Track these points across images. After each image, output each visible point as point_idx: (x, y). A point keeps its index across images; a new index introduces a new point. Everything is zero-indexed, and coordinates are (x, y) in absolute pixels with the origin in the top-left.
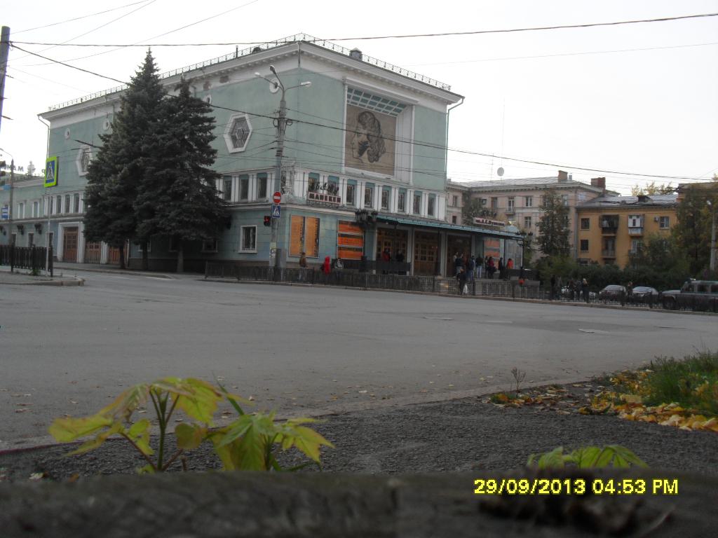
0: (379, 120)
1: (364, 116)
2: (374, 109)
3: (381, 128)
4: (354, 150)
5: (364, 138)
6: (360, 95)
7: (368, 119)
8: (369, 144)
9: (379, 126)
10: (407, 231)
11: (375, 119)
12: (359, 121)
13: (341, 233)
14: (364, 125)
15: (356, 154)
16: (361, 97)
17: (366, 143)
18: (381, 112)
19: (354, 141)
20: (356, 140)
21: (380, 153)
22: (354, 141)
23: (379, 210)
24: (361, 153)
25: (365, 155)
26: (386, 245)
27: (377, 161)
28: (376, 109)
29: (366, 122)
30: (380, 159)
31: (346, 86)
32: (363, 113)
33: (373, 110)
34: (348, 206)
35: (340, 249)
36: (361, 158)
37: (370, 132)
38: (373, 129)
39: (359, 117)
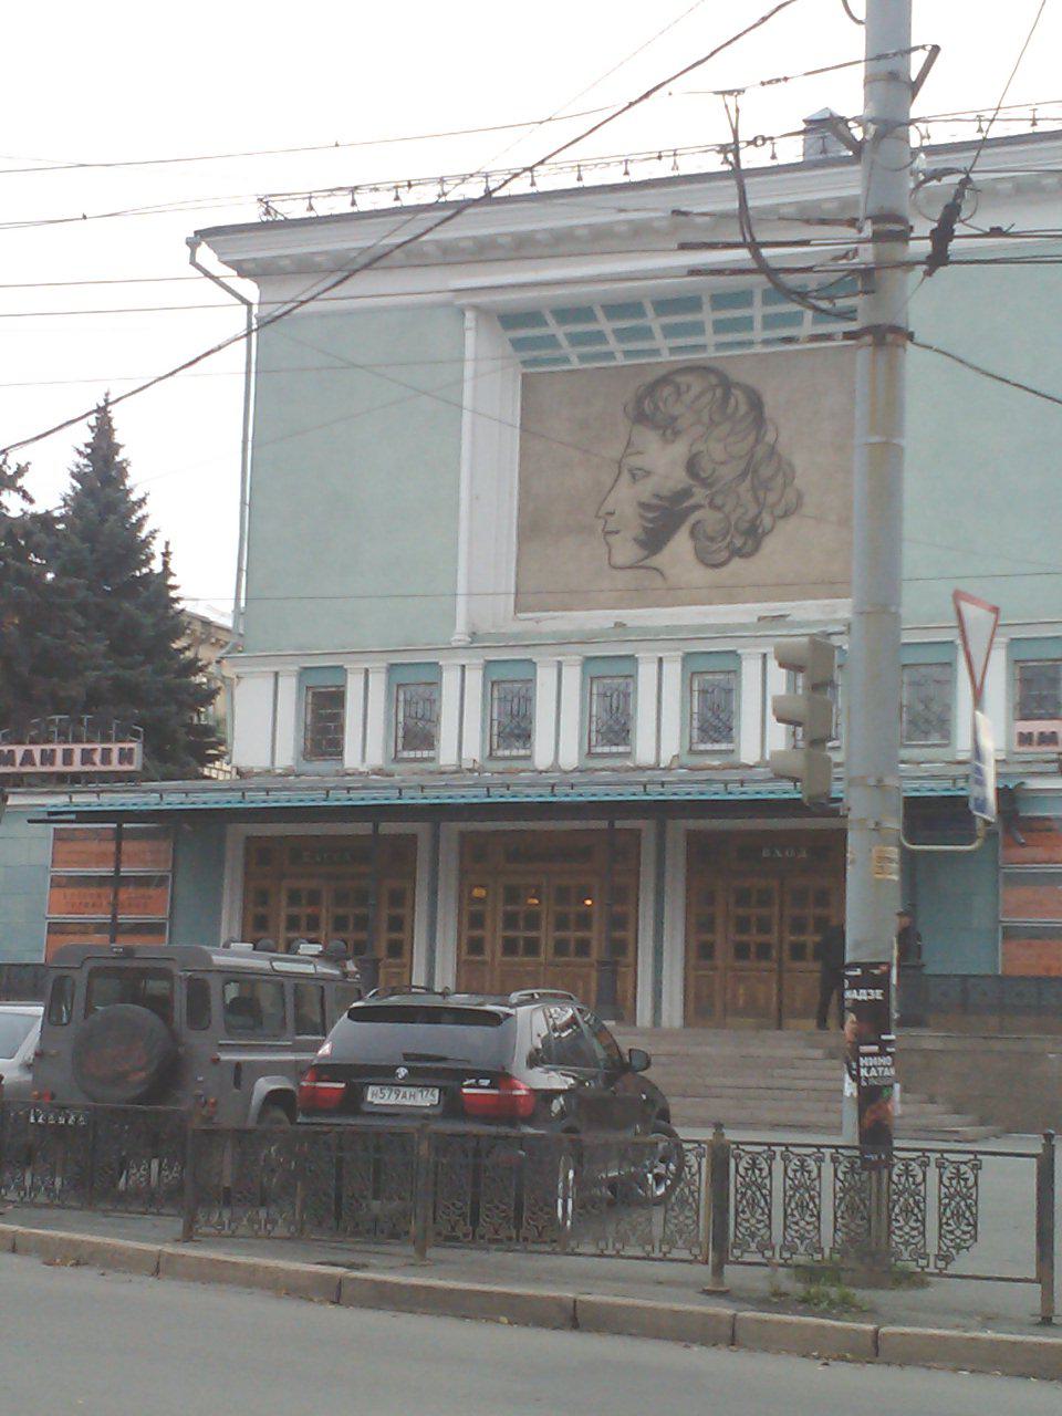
0: (750, 381)
1: (667, 391)
2: (710, 346)
3: (768, 411)
4: (613, 539)
5: (680, 478)
6: (749, 304)
7: (687, 398)
8: (700, 495)
9: (756, 403)
10: (413, 839)
11: (727, 385)
12: (641, 417)
13: (63, 871)
14: (669, 429)
15: (626, 551)
16: (707, 316)
17: (686, 493)
18: (758, 349)
19: (608, 507)
20: (626, 499)
21: (767, 520)
22: (608, 507)
23: (665, 760)
24: (654, 539)
25: (681, 543)
26: (294, 898)
27: (738, 553)
28: (720, 346)
29: (677, 410)
30: (770, 545)
31: (469, 315)
32: (664, 380)
33: (711, 353)
34: (501, 766)
35: (55, 929)
36: (658, 560)
37: (700, 447)
38: (725, 428)
39: (639, 401)
